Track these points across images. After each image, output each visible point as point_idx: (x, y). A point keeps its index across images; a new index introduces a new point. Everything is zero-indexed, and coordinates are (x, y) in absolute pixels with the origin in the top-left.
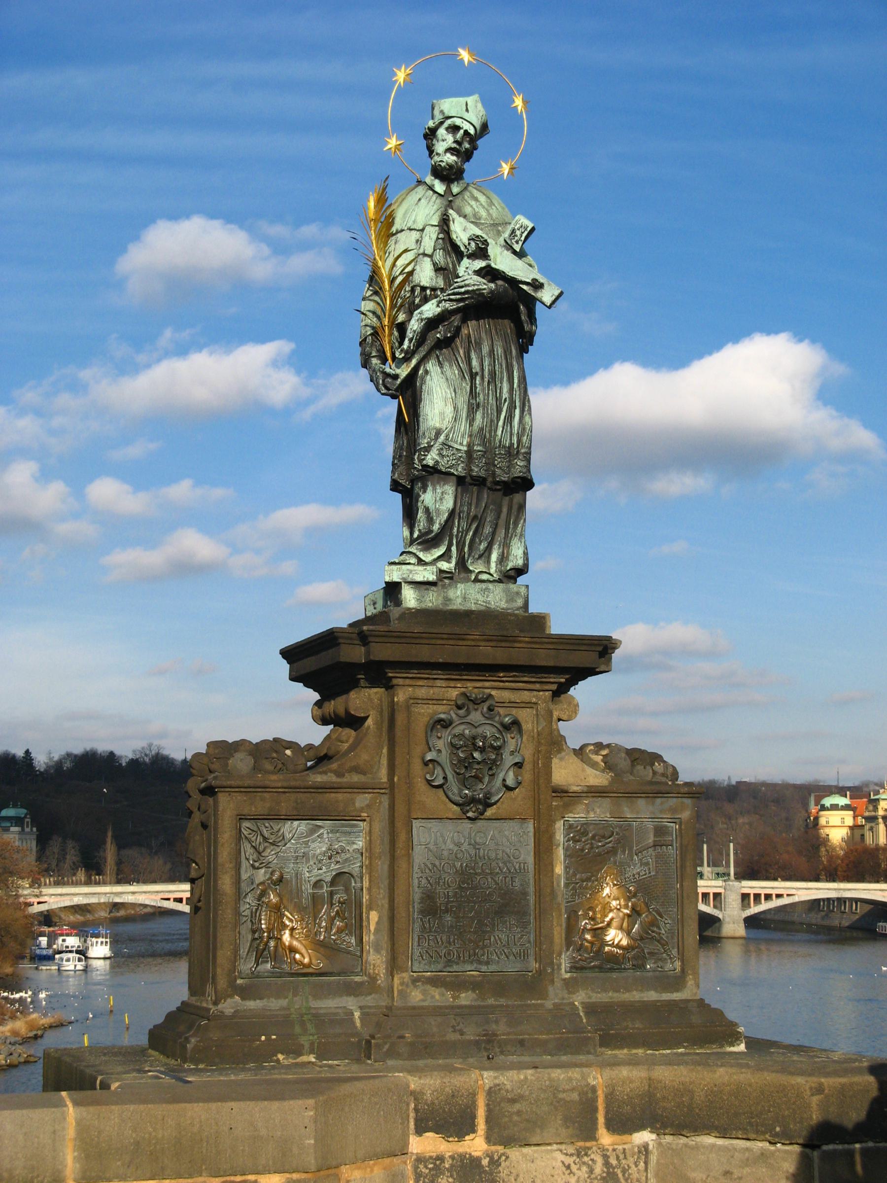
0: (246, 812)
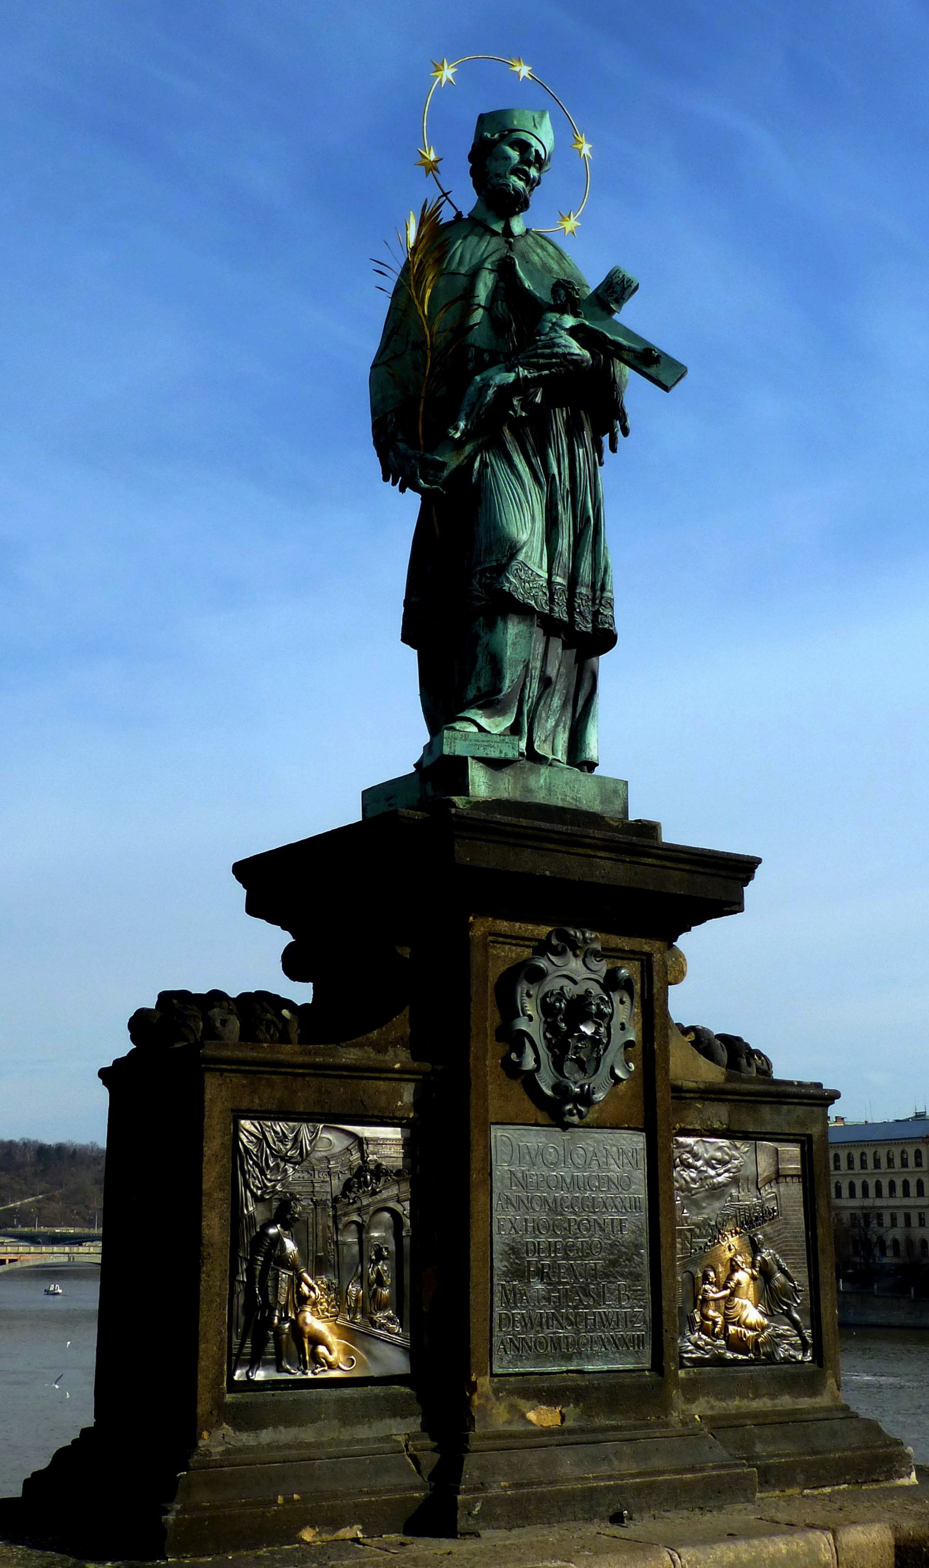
0: (244, 1105)
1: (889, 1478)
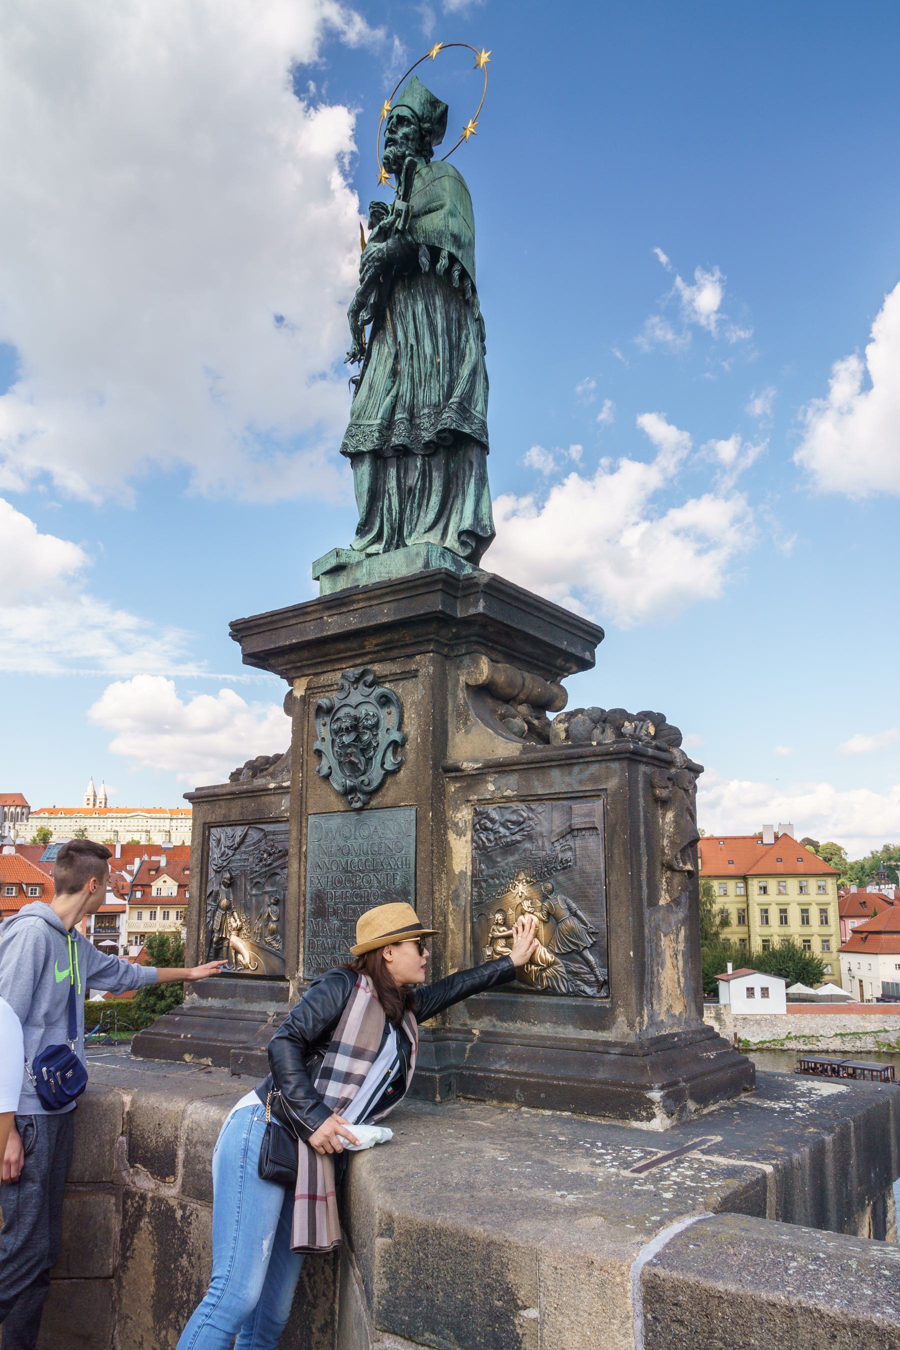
1: (624, 1118)
